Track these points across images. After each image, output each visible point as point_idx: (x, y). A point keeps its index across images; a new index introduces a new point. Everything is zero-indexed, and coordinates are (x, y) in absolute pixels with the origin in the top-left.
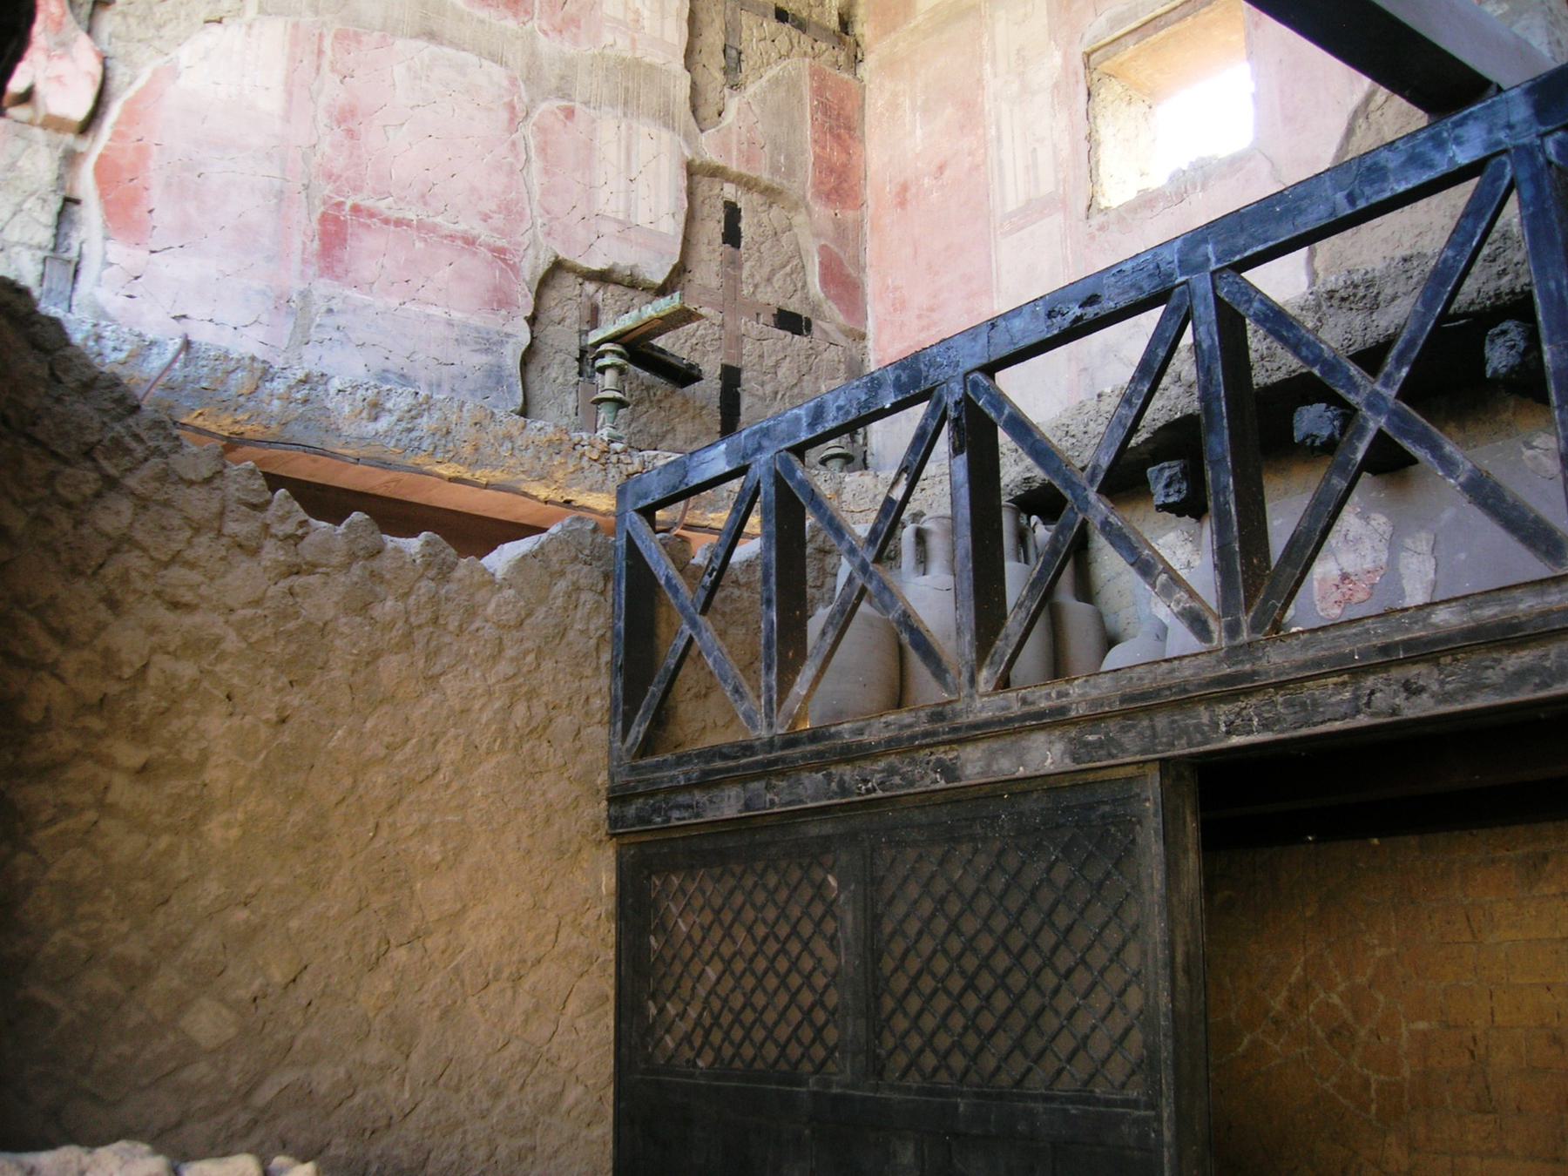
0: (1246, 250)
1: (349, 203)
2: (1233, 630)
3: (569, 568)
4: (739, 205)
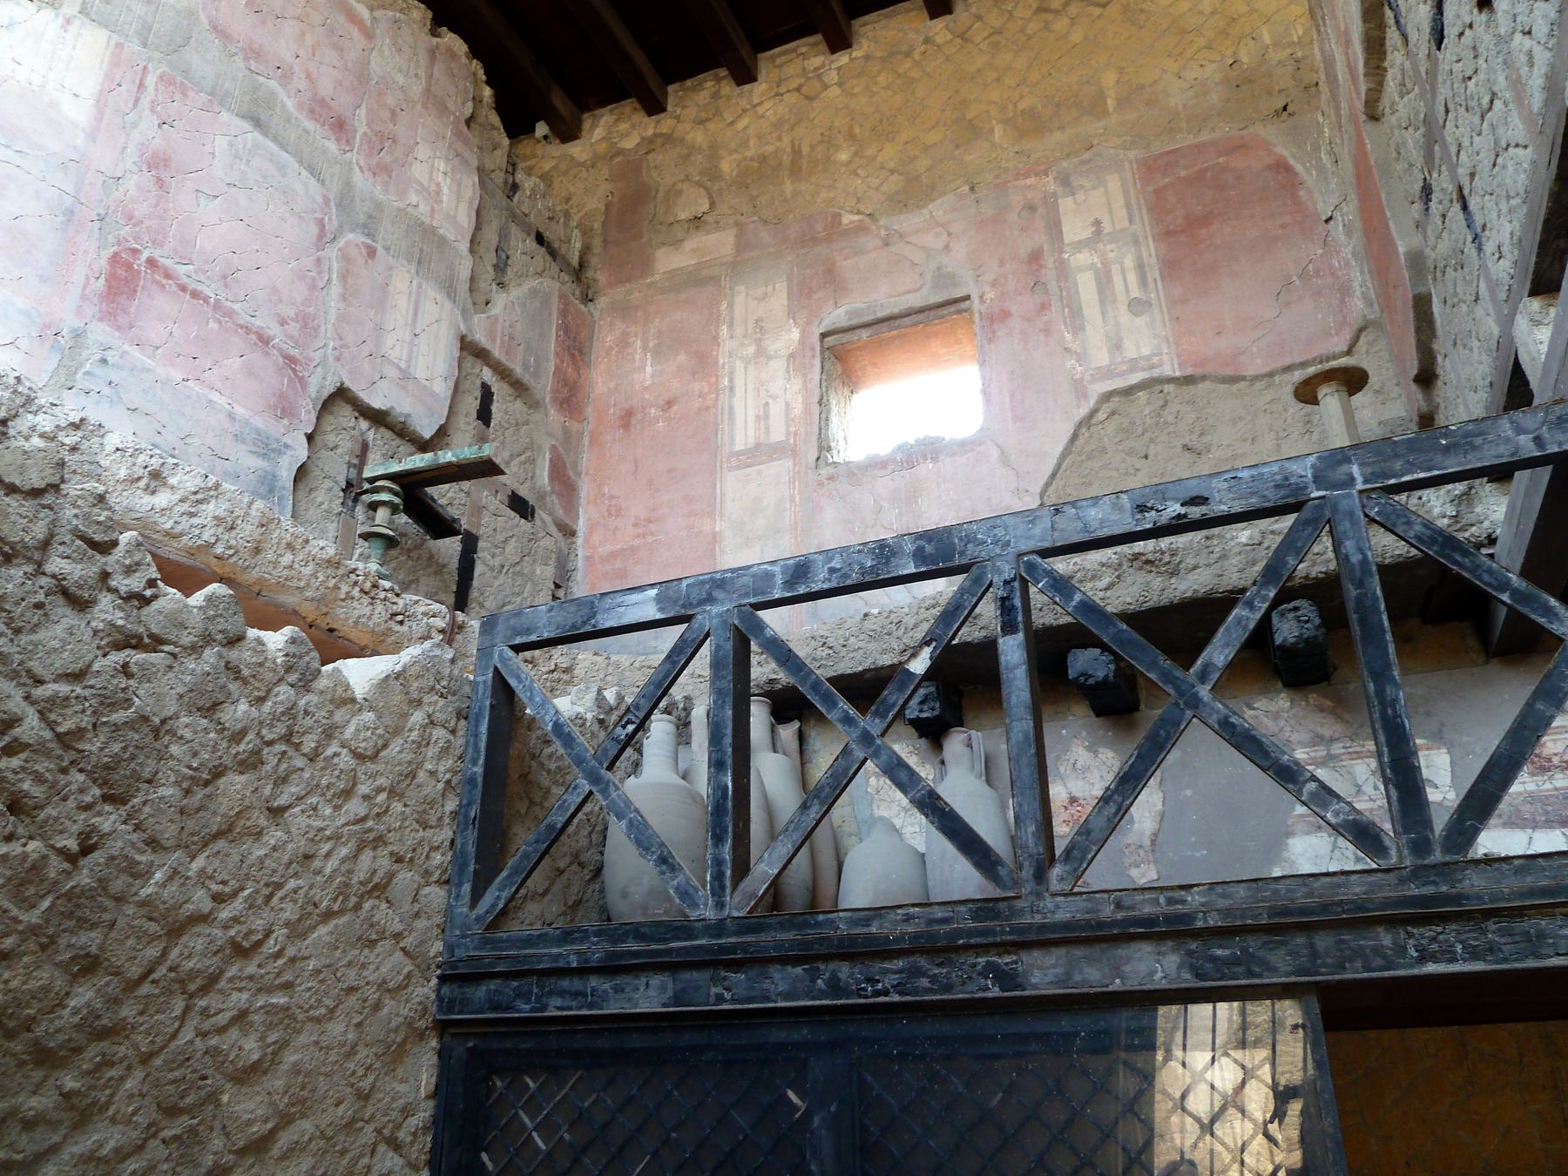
0: (1402, 475)
1: (145, 255)
2: (1421, 846)
3: (426, 699)
4: (493, 389)
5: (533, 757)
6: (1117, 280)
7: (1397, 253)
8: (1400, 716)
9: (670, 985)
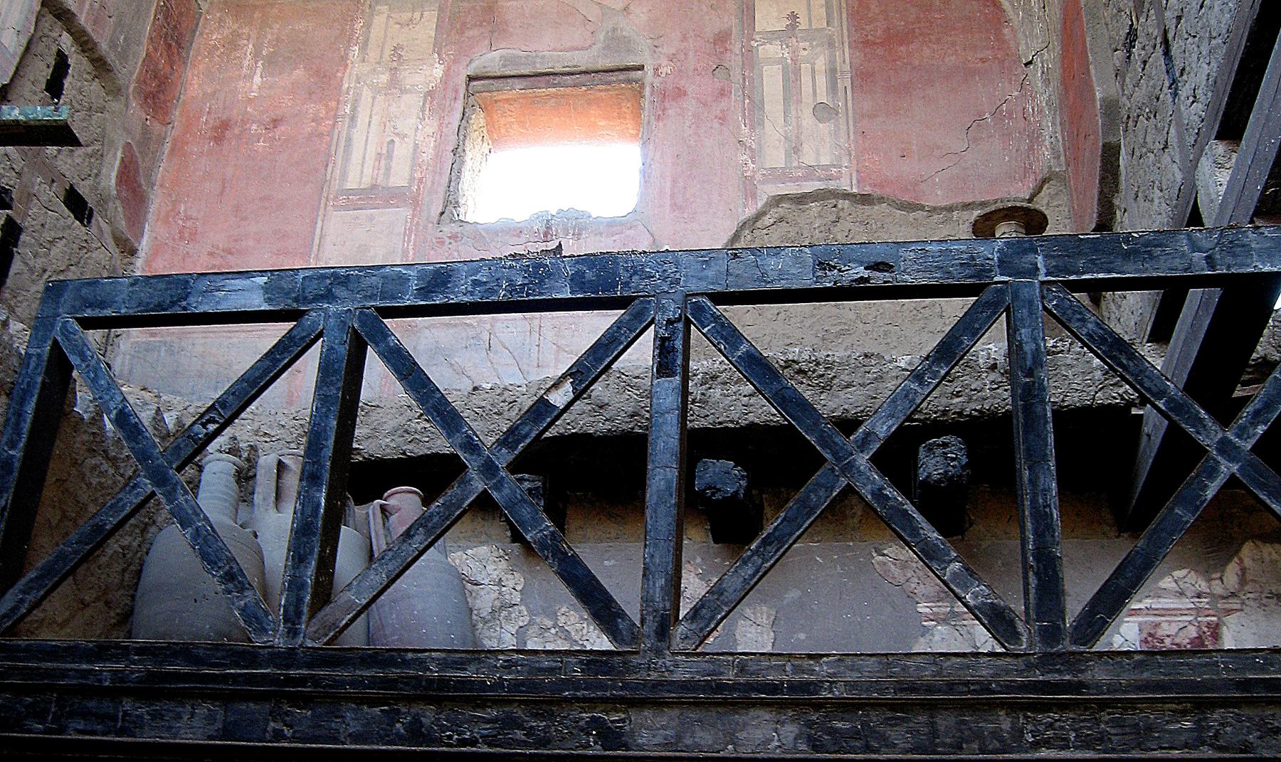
0: (1083, 273)
2: (1051, 634)
4: (70, 61)
5: (75, 463)
6: (806, 79)
7: (1093, 99)
8: (1049, 506)
9: (220, 716)
